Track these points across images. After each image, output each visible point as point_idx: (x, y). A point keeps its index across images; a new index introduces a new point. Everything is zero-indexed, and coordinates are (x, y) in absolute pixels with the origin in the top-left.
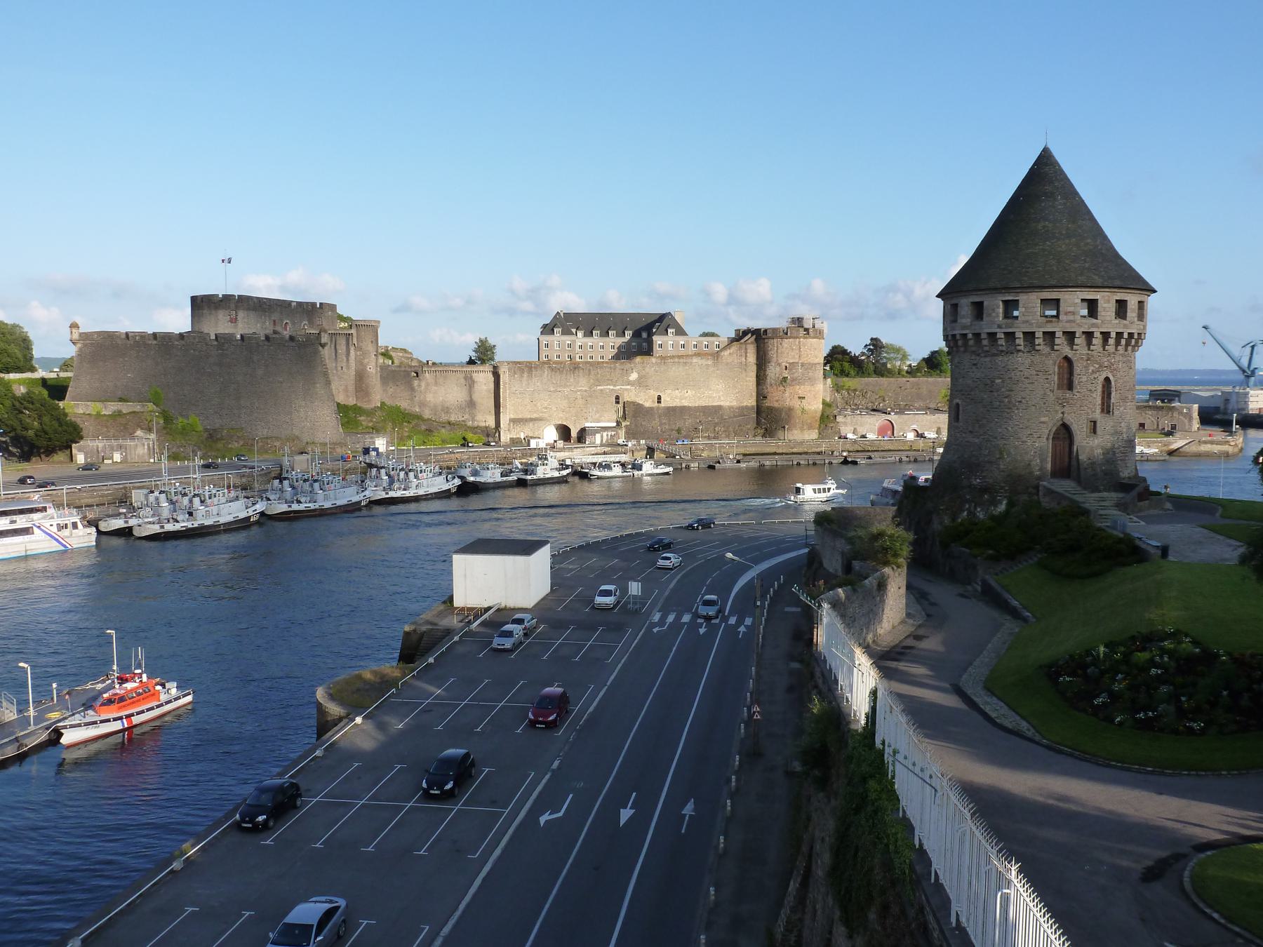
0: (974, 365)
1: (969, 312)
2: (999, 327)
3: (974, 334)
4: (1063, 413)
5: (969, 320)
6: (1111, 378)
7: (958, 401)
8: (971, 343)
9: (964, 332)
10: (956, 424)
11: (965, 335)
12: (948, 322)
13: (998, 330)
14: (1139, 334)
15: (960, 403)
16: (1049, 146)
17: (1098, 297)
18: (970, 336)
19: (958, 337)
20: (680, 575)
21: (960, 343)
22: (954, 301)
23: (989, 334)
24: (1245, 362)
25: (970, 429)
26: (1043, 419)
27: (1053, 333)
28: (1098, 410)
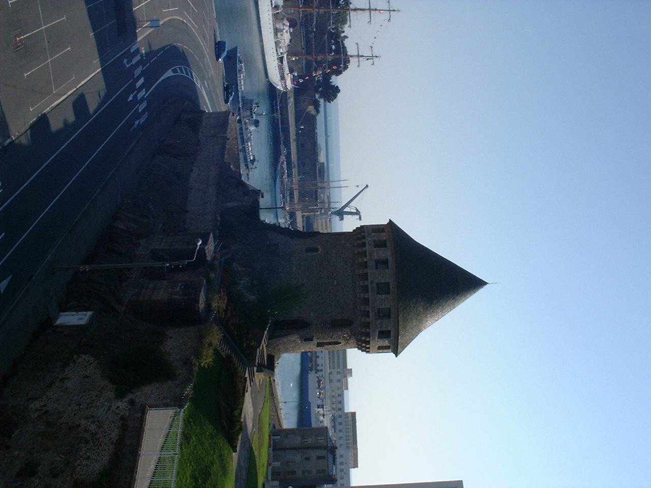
0: (346, 262)
1: (381, 258)
2: (372, 282)
3: (366, 262)
4: (316, 324)
5: (376, 258)
6: (340, 345)
7: (320, 250)
9: (368, 255)
10: (304, 250)
11: (365, 252)
12: (375, 239)
13: (369, 281)
14: (369, 351)
15: (319, 252)
16: (488, 285)
17: (392, 338)
18: (365, 260)
19: (364, 249)
20: (169, 18)
21: (360, 250)
22: (388, 244)
23: (367, 274)
25: (301, 263)
26: (312, 314)
27: (369, 317)
28: (318, 341)
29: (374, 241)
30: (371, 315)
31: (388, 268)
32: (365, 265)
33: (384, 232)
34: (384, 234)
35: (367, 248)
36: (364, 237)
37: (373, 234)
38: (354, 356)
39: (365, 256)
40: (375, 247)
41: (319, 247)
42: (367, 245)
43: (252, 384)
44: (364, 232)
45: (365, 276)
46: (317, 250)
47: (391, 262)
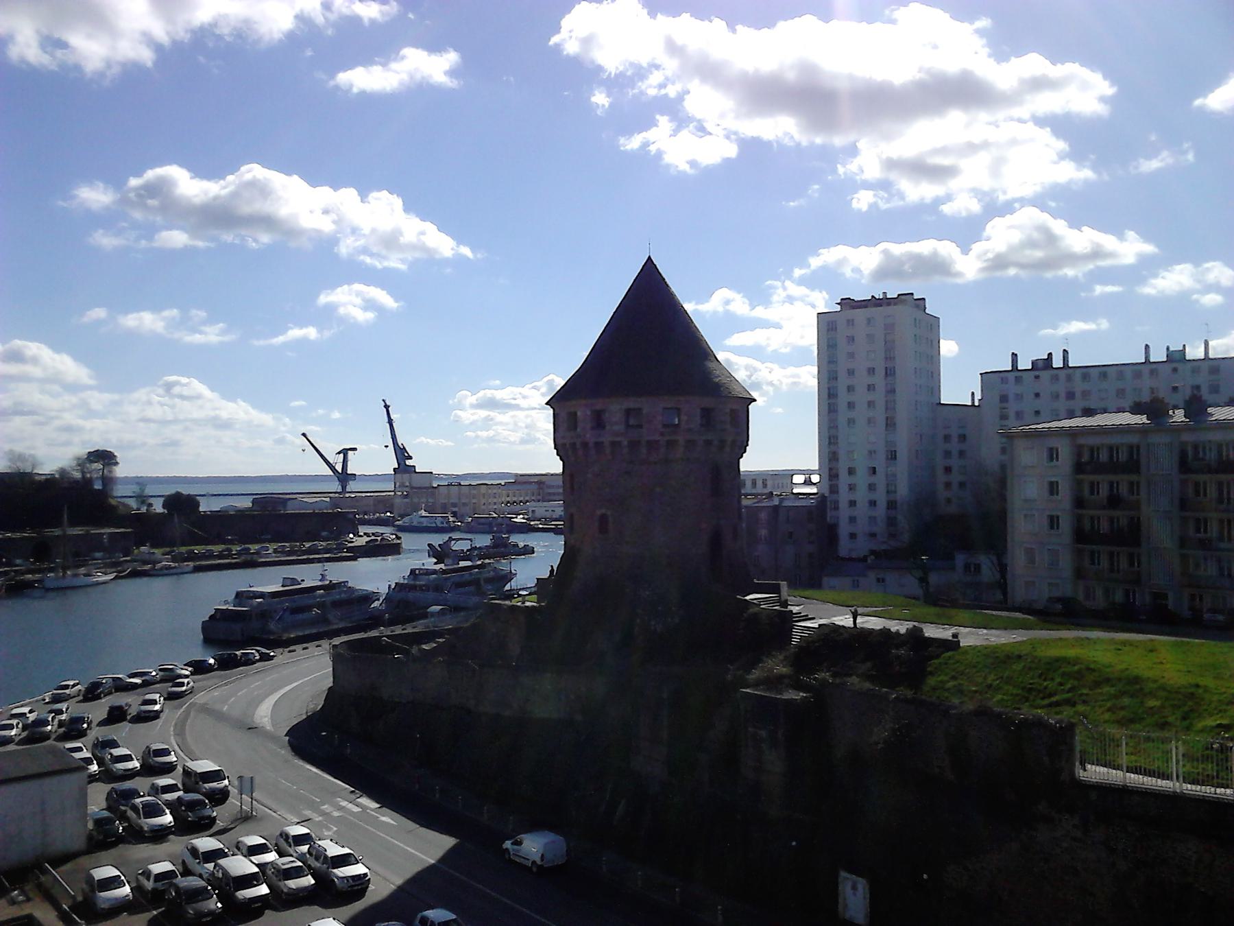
2: (662, 434)
7: (603, 511)
8: (608, 451)
9: (618, 439)
11: (613, 444)
15: (609, 513)
18: (626, 443)
21: (608, 451)
22: (598, 407)
24: (339, 468)
29: (593, 428)
30: (709, 438)
31: (640, 409)
32: (634, 445)
33: (575, 414)
34: (579, 414)
35: (606, 439)
36: (585, 445)
37: (578, 430)
38: (749, 463)
39: (619, 443)
40: (604, 427)
41: (599, 512)
42: (600, 440)
43: (810, 617)
44: (574, 444)
45: (652, 445)
46: (603, 519)
47: (632, 403)
